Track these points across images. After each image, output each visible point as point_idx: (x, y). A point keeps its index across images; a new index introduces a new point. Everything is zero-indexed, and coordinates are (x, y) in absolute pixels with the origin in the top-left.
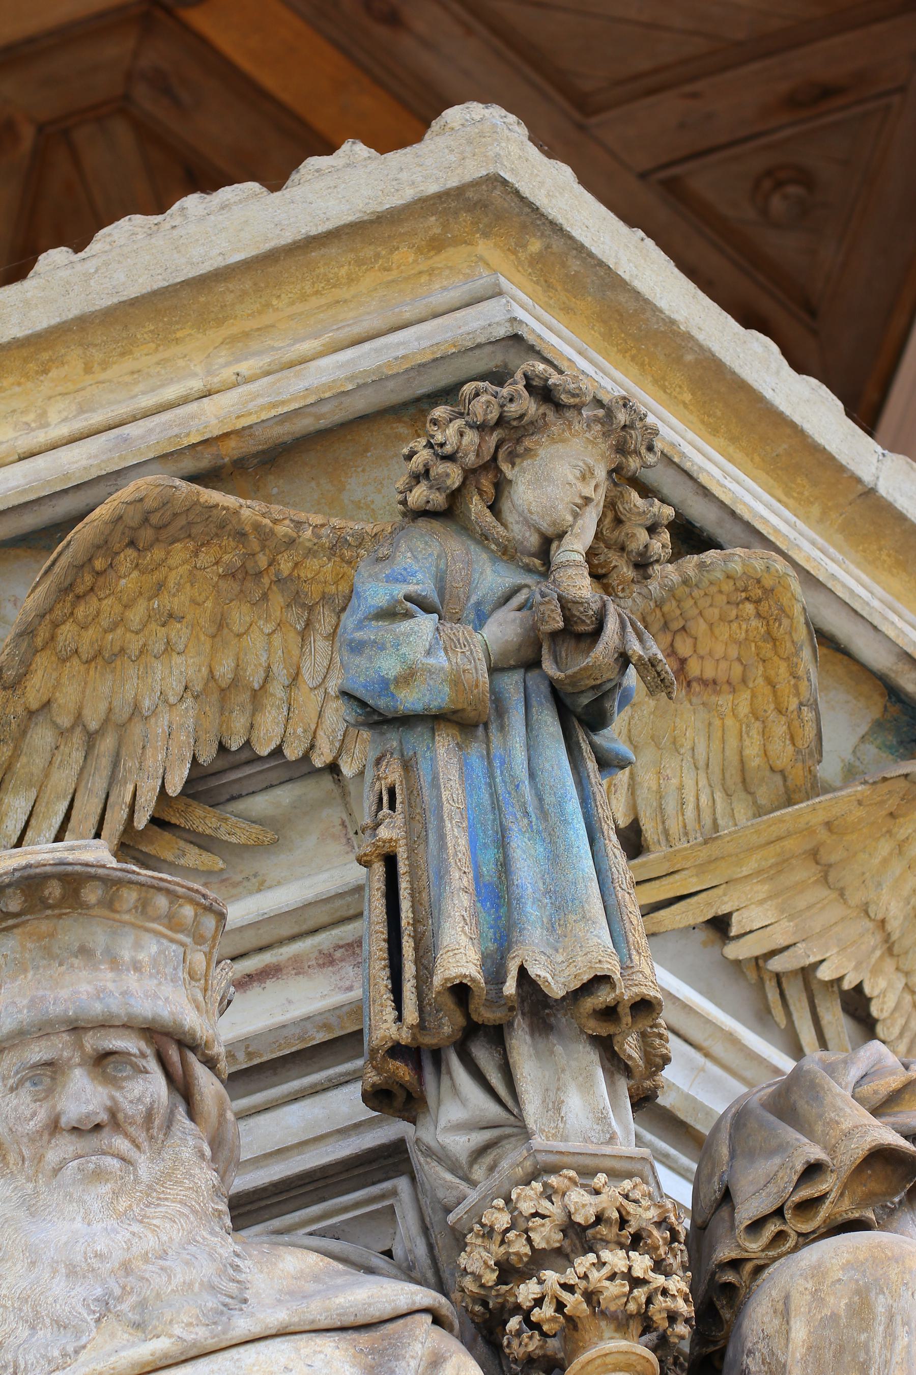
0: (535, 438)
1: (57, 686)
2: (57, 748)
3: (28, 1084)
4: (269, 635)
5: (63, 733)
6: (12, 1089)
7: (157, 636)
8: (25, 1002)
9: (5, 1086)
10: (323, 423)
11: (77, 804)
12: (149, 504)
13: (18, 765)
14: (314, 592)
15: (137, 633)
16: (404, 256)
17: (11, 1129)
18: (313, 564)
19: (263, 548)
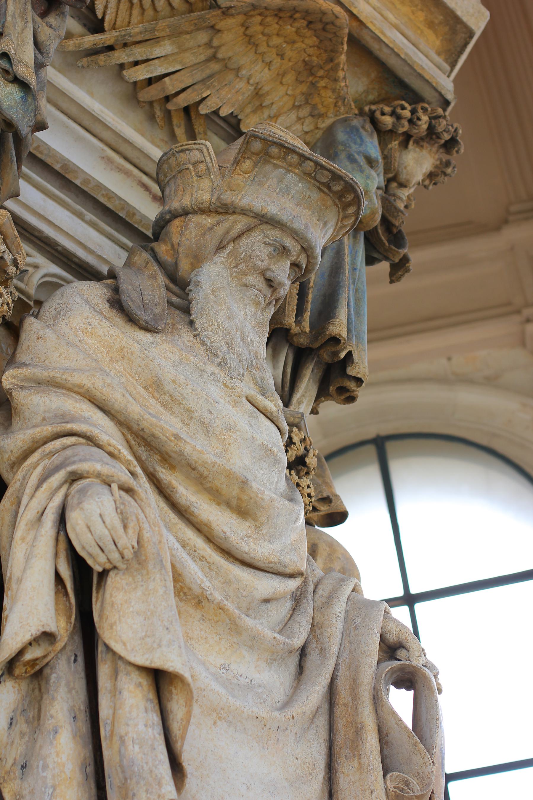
0: (428, 145)
1: (229, 30)
2: (199, 46)
3: (272, 248)
4: (287, 94)
5: (209, 44)
6: (265, 243)
7: (272, 55)
8: (304, 222)
9: (263, 239)
10: (377, 53)
11: (182, 72)
12: (338, 22)
13: (184, 36)
14: (316, 100)
15: (268, 46)
16: (421, 16)
17: (251, 255)
18: (329, 93)
19: (328, 71)
